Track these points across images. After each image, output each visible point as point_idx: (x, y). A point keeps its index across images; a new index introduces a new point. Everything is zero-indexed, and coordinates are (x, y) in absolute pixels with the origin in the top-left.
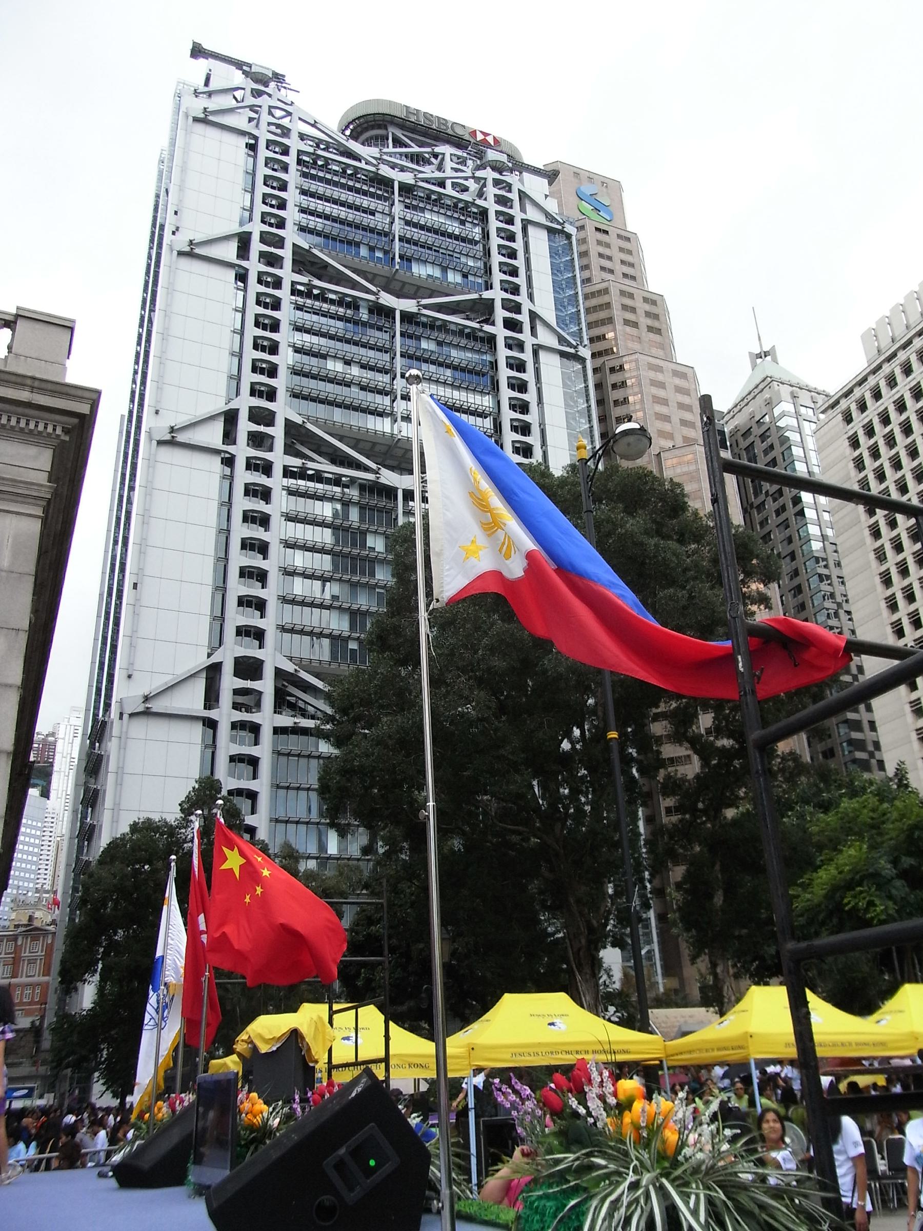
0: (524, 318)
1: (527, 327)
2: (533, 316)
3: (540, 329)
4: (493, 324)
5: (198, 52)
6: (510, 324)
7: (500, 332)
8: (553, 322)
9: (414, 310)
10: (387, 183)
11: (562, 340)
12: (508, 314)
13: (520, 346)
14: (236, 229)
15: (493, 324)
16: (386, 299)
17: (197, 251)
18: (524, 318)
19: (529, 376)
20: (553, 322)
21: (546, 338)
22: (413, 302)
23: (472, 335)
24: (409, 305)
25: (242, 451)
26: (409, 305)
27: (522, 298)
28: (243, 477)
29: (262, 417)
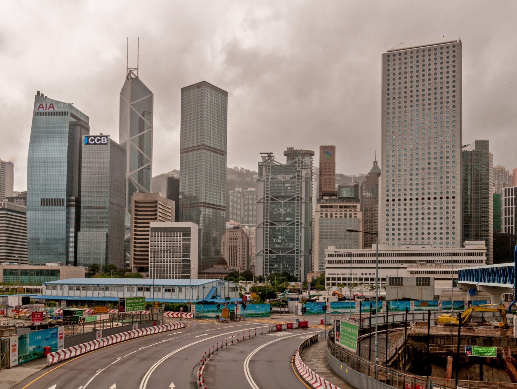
5: (261, 153)
16: (281, 201)
26: (284, 201)
29: (267, 222)
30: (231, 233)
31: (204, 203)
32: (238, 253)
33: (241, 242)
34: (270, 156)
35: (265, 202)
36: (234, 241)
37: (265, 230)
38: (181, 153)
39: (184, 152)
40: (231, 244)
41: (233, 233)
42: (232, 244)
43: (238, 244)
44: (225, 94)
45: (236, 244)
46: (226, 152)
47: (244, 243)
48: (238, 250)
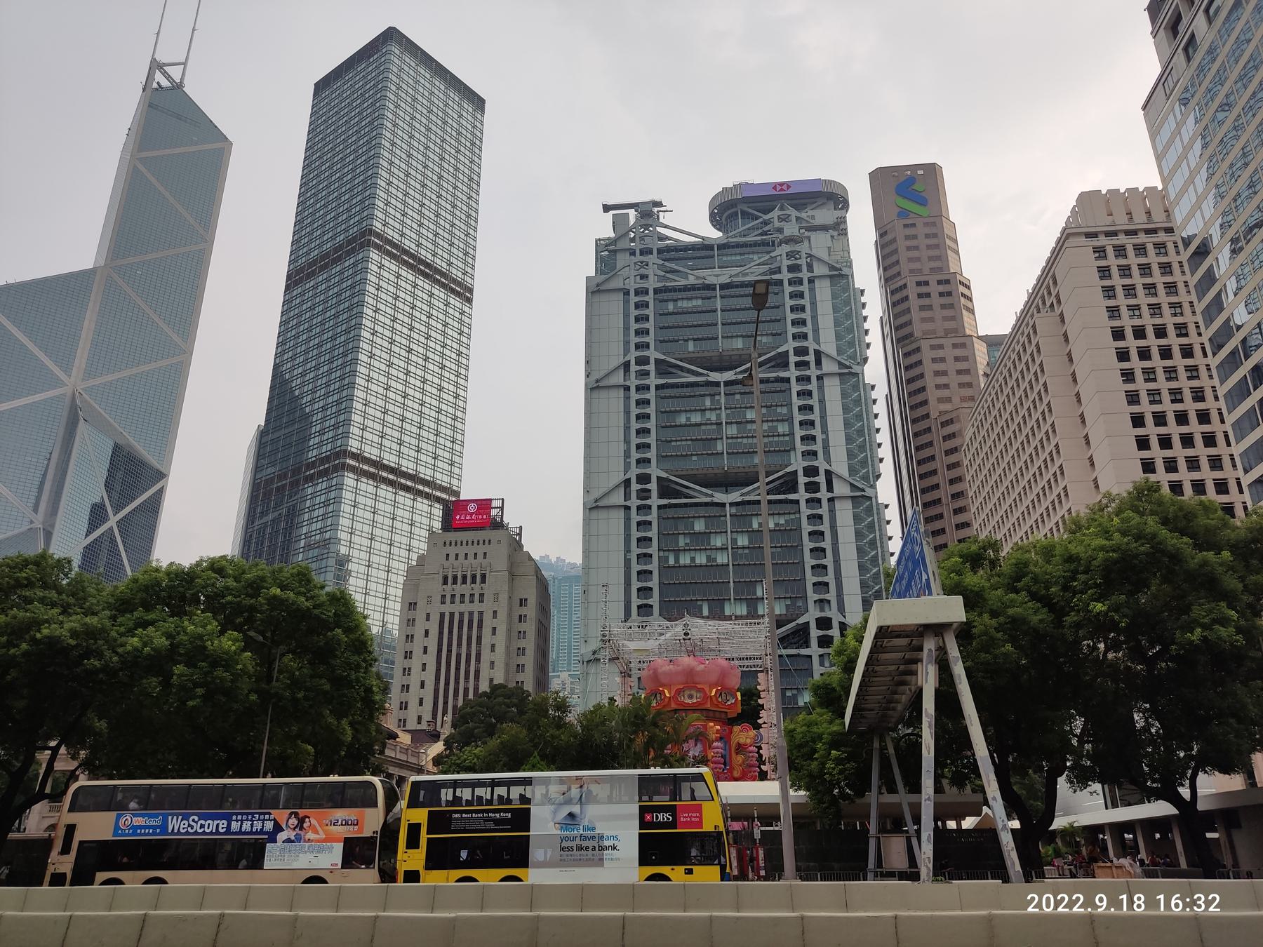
2: (818, 354)
5: (607, 208)
7: (792, 373)
8: (834, 353)
9: (733, 378)
10: (711, 287)
11: (841, 364)
14: (621, 360)
16: (714, 376)
17: (601, 384)
20: (834, 353)
22: (732, 372)
24: (729, 376)
25: (634, 502)
26: (729, 376)
27: (811, 344)
28: (635, 517)
30: (452, 551)
31: (354, 456)
32: (486, 656)
33: (504, 597)
34: (648, 212)
35: (633, 382)
36: (466, 589)
37: (635, 517)
38: (288, 288)
39: (296, 283)
40: (447, 608)
41: (462, 550)
42: (457, 608)
43: (487, 607)
44: (479, 103)
45: (476, 607)
46: (471, 291)
47: (523, 602)
48: (486, 640)
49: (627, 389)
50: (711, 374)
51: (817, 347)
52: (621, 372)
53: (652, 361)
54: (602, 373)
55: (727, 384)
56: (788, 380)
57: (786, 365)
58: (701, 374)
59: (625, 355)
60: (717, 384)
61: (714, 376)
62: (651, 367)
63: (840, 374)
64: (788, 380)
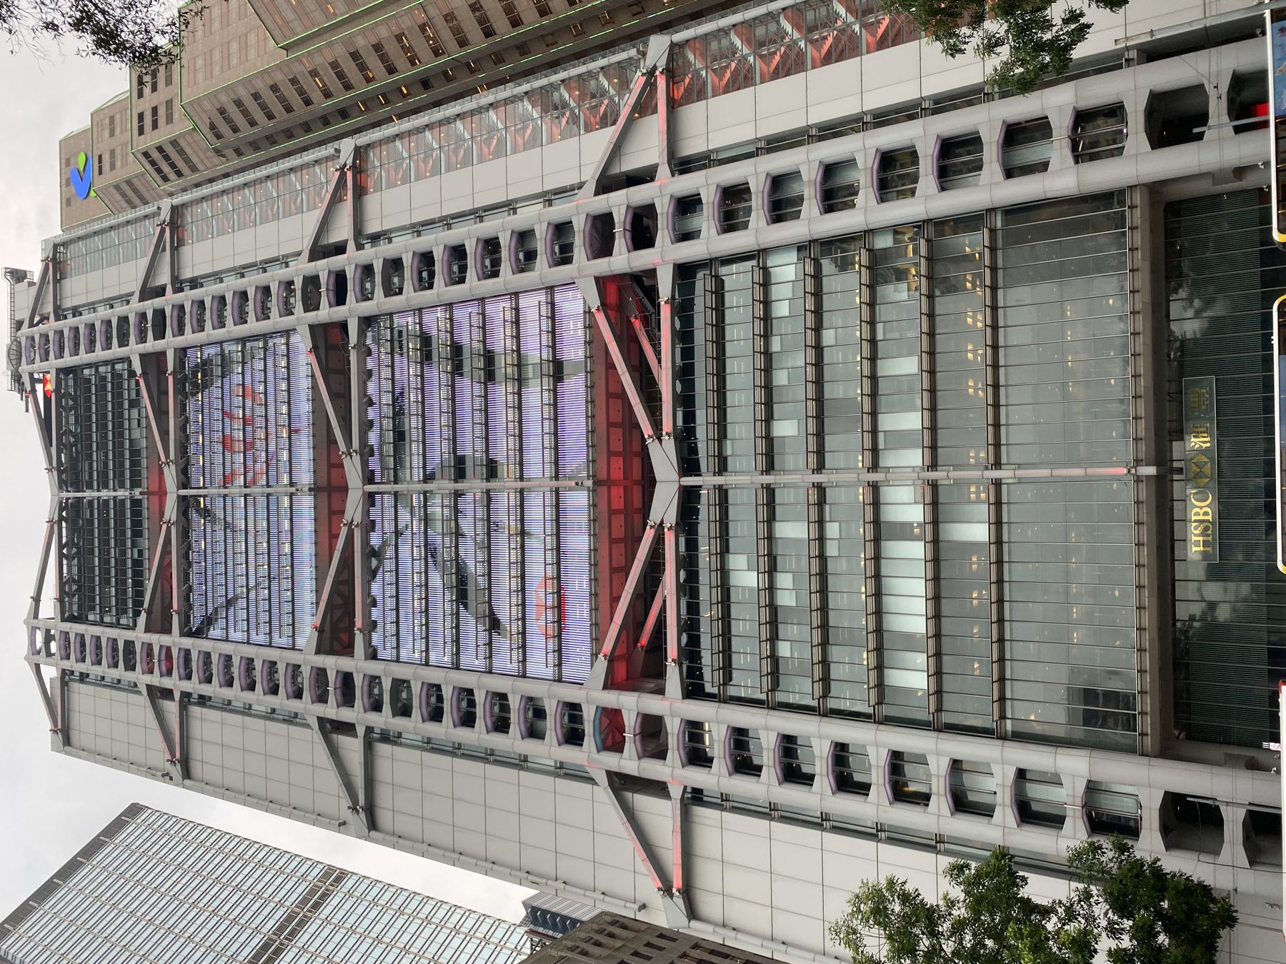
0: (619, 203)
1: (639, 194)
2: (607, 184)
3: (631, 163)
4: (652, 273)
6: (642, 235)
7: (663, 256)
8: (605, 138)
9: (669, 444)
11: (644, 107)
12: (620, 243)
13: (687, 205)
14: (603, 793)
15: (652, 273)
16: (664, 506)
17: (677, 882)
18: (619, 203)
19: (755, 173)
20: (605, 138)
21: (648, 147)
22: (654, 448)
23: (683, 309)
24: (663, 457)
26: (663, 457)
49: (696, 797)
50: (655, 516)
51: (591, 187)
52: (644, 803)
53: (613, 699)
54: (644, 867)
55: (689, 465)
56: (685, 272)
57: (643, 282)
58: (659, 540)
59: (591, 780)
60: (689, 498)
61: (664, 506)
62: (631, 704)
63: (673, 105)
64: (685, 272)
